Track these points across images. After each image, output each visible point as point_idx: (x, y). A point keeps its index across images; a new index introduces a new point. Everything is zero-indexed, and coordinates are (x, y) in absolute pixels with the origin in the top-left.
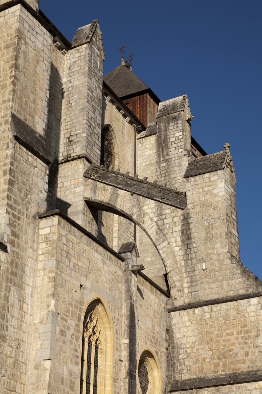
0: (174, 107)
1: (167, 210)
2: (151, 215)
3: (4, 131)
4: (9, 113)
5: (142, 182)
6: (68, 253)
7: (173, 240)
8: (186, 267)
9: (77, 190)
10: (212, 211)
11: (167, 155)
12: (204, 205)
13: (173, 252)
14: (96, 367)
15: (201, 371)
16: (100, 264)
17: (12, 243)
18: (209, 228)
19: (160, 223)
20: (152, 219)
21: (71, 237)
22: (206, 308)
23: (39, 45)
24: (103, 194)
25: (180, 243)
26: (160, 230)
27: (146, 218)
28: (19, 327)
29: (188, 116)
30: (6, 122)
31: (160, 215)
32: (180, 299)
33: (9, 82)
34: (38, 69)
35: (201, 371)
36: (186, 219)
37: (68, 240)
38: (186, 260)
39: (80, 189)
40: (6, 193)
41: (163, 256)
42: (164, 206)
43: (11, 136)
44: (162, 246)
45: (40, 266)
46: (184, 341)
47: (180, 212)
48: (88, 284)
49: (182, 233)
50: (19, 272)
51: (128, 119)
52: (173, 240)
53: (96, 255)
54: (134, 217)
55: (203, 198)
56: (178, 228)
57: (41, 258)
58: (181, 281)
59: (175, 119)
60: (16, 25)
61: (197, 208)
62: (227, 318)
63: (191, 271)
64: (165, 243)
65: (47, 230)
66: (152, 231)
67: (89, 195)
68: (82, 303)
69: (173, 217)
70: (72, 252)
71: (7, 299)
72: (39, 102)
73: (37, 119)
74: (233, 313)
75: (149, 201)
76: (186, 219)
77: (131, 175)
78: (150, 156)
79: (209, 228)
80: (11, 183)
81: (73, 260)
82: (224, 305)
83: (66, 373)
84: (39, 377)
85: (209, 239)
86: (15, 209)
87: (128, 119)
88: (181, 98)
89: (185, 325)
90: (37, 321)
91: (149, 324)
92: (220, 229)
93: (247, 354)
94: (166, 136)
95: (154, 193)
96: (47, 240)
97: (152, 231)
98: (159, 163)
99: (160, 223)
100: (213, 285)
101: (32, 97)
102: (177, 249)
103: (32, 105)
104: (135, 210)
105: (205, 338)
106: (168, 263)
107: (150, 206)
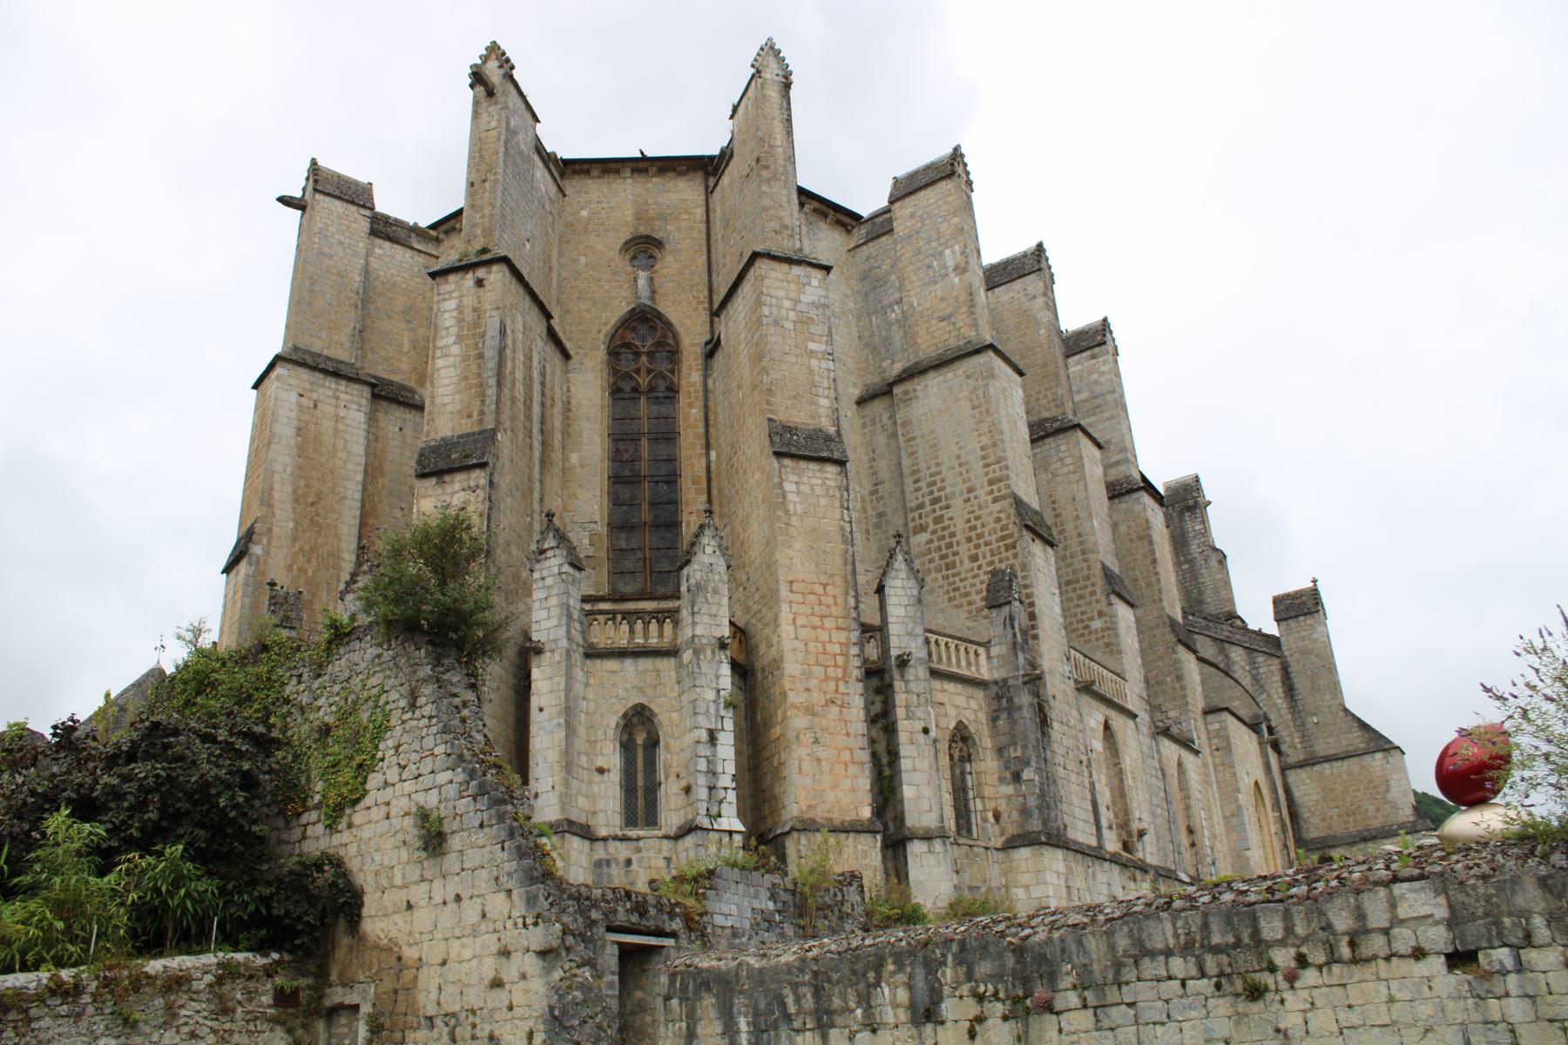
8: (1294, 720)
10: (1313, 659)
12: (1305, 652)
13: (1276, 705)
15: (1330, 828)
22: (1326, 765)
27: (1236, 667)
31: (1252, 663)
32: (1294, 757)
35: (1330, 828)
38: (1293, 714)
46: (1305, 799)
47: (1276, 661)
55: (1301, 644)
56: (1277, 678)
58: (1291, 735)
61: (1297, 656)
62: (1350, 774)
63: (1302, 728)
66: (1246, 681)
74: (1356, 768)
82: (1346, 762)
89: (1305, 785)
93: (1378, 810)
97: (1246, 681)
100: (1331, 740)
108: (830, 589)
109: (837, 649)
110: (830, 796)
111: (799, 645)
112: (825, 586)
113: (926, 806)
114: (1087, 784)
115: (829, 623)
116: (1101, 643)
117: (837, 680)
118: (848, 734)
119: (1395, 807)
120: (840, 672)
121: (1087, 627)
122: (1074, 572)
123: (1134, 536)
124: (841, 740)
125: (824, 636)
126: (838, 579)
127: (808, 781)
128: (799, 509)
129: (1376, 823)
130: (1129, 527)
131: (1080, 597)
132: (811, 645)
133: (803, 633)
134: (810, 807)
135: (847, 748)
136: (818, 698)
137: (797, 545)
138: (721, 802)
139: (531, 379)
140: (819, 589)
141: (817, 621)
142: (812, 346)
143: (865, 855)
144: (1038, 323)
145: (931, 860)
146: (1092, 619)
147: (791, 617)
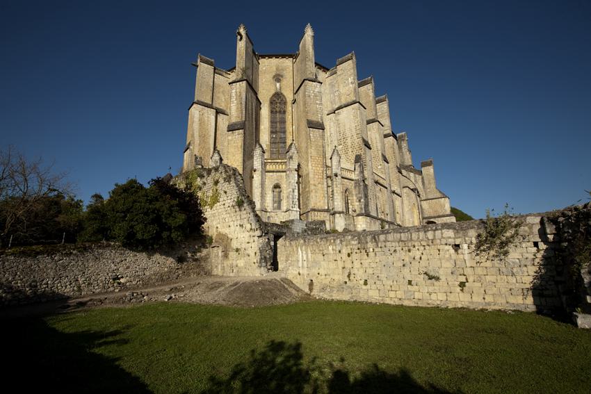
0: (402, 136)
1: (417, 176)
18: (429, 180)
26: (415, 181)
36: (423, 178)
56: (421, 180)
59: (403, 140)
63: (425, 191)
66: (413, 181)
69: (419, 177)
76: (423, 178)
79: (429, 180)
85: (429, 183)
89: (425, 205)
92: (433, 181)
97: (413, 181)
105: (430, 207)
107: (412, 174)
110: (318, 204)
119: (446, 211)
129: (441, 214)
137: (313, 148)
143: (326, 217)
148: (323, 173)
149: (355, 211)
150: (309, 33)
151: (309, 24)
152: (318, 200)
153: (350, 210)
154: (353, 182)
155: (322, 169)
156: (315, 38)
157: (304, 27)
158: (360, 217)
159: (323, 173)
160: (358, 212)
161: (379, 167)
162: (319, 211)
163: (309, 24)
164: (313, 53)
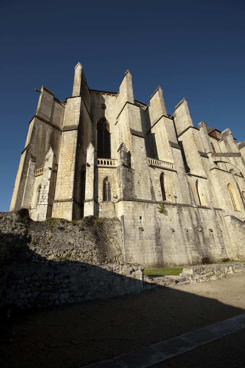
0: (226, 132)
1: (236, 158)
2: (232, 160)
3: (197, 155)
4: (197, 151)
5: (227, 153)
6: (220, 176)
7: (240, 164)
9: (211, 160)
11: (228, 144)
13: (241, 167)
14: (233, 197)
16: (227, 176)
17: (208, 177)
19: (235, 162)
20: (233, 161)
21: (219, 172)
23: (197, 134)
24: (218, 159)
25: (243, 165)
26: (236, 163)
28: (215, 194)
29: (231, 133)
30: (197, 153)
31: (235, 160)
33: (195, 144)
34: (199, 139)
37: (219, 173)
39: (212, 159)
40: (203, 168)
41: (239, 169)
42: (235, 158)
43: (199, 155)
44: (238, 167)
45: (214, 180)
47: (240, 158)
48: (226, 181)
49: (242, 162)
50: (211, 183)
51: (215, 139)
52: (240, 164)
53: (225, 174)
54: (228, 162)
57: (214, 178)
59: (227, 135)
60: (192, 132)
64: (238, 166)
65: (214, 172)
66: (234, 164)
67: (214, 160)
68: (226, 185)
70: (220, 175)
71: (210, 189)
72: (202, 146)
73: (203, 150)
75: (230, 157)
77: (220, 153)
78: (223, 146)
80: (203, 165)
81: (221, 177)
83: (228, 200)
84: (222, 203)
86: (205, 170)
87: (215, 139)
88: (227, 129)
90: (218, 191)
91: (241, 185)
94: (226, 140)
95: (231, 155)
96: (214, 174)
97: (234, 164)
98: (226, 146)
99: (235, 162)
101: (200, 146)
102: (242, 166)
103: (200, 147)
104: (227, 161)
106: (241, 170)
107: (231, 159)
108: (70, 154)
109: (69, 165)
110: (63, 195)
111: (62, 166)
112: (69, 153)
113: (90, 195)
114: (149, 186)
115: (69, 160)
116: (169, 158)
117: (68, 171)
118: (69, 182)
120: (69, 170)
121: (167, 155)
122: (164, 145)
123: (190, 137)
124: (67, 183)
125: (67, 163)
126: (72, 152)
127: (59, 192)
128: (66, 140)
130: (189, 136)
131: (166, 150)
132: (64, 166)
133: (63, 163)
134: (58, 198)
135: (68, 184)
136: (64, 175)
137: (64, 147)
138: (44, 199)
139: (45, 135)
140: (67, 154)
141: (66, 160)
142: (76, 111)
143: (68, 206)
144: (158, 100)
145: (89, 206)
146: (168, 153)
147: (61, 161)
148: (71, 166)
149: (116, 198)
150: (78, 69)
151: (79, 63)
152: (63, 192)
153: (112, 197)
154: (116, 170)
155: (71, 162)
156: (83, 71)
157: (75, 65)
158: (120, 203)
159: (71, 166)
160: (119, 198)
161: (168, 154)
162: (62, 201)
163: (79, 63)
164: (80, 79)
